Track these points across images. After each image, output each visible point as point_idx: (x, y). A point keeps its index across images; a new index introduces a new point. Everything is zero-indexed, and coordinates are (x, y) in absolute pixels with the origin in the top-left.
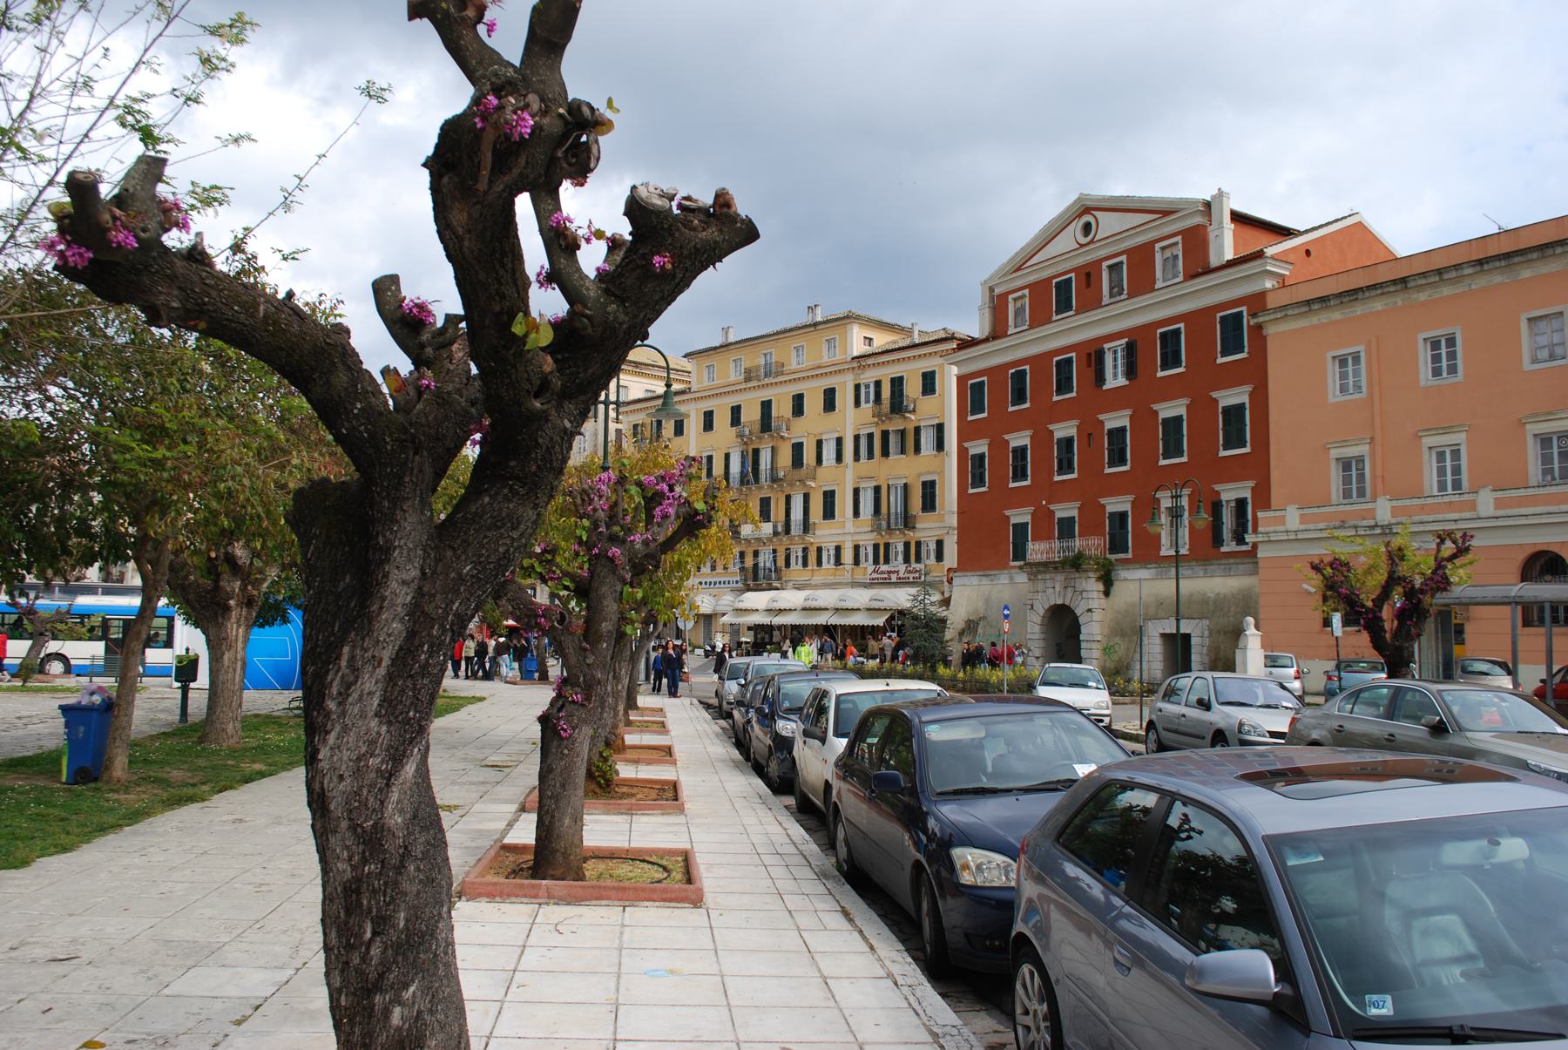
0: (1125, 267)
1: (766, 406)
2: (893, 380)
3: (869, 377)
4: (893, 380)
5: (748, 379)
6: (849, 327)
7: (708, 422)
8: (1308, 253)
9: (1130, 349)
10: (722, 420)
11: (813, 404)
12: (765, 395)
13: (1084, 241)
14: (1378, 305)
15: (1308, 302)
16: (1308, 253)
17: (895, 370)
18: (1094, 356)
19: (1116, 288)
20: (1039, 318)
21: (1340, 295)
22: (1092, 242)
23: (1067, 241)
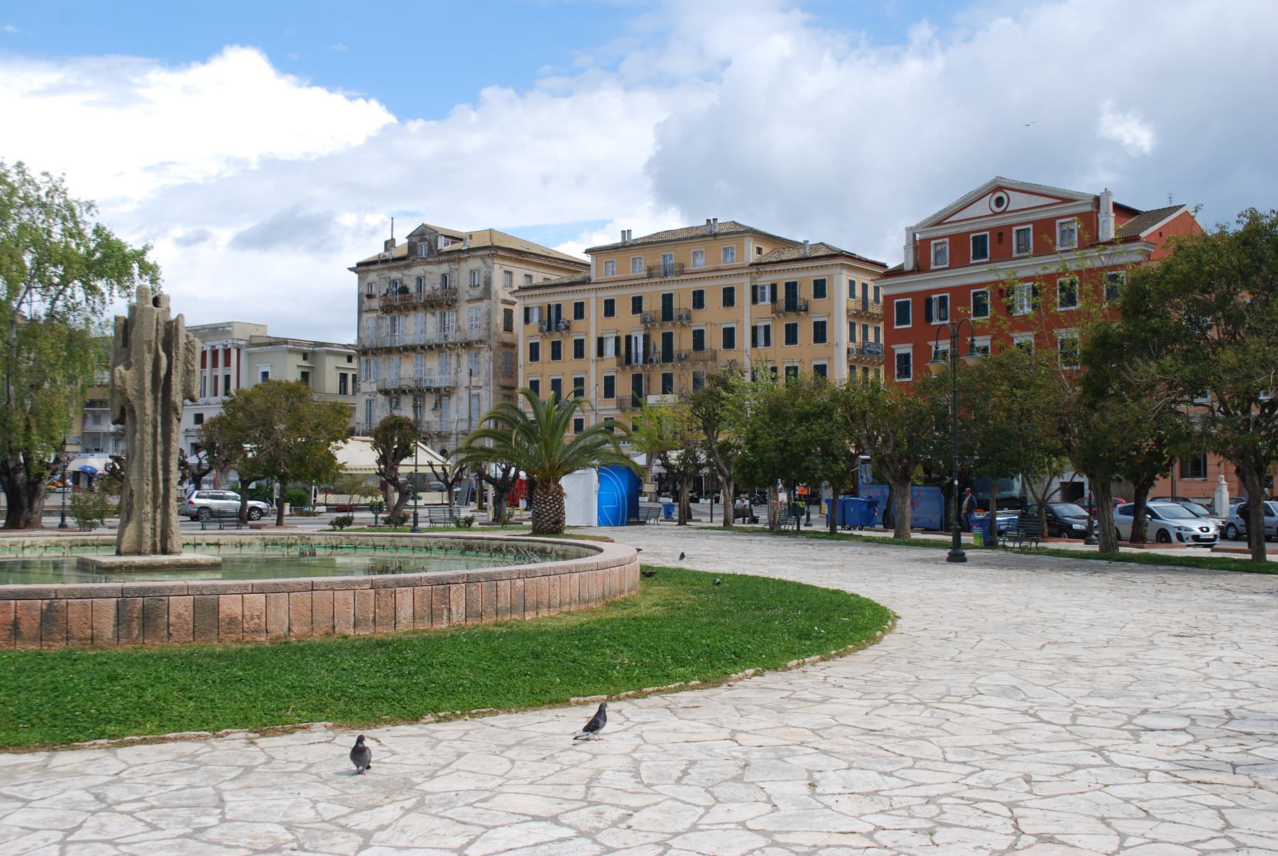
0: (1031, 233)
1: (667, 299)
2: (787, 285)
3: (765, 280)
4: (787, 285)
5: (650, 276)
6: (746, 239)
7: (609, 308)
8: (1161, 234)
11: (714, 299)
12: (667, 289)
13: (997, 210)
16: (1161, 234)
17: (790, 277)
18: (1003, 291)
19: (1022, 247)
20: (958, 261)
23: (983, 208)
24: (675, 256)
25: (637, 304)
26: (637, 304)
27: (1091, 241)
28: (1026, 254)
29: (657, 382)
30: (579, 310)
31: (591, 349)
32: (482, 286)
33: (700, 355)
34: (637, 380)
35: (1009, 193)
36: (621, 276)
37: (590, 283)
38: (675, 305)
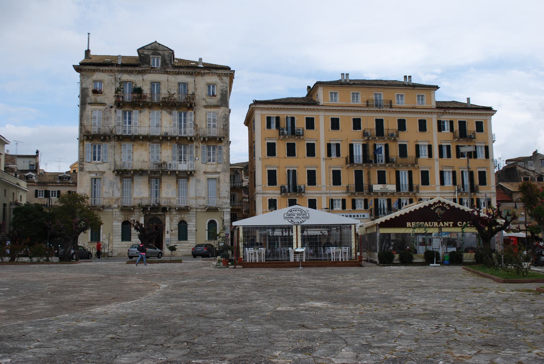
1: (379, 123)
2: (460, 122)
4: (460, 122)
7: (335, 124)
10: (346, 124)
11: (412, 125)
12: (380, 116)
17: (462, 118)
24: (384, 95)
25: (357, 124)
26: (357, 124)
29: (375, 177)
30: (310, 123)
31: (321, 150)
32: (219, 97)
33: (404, 160)
34: (359, 175)
36: (344, 103)
37: (319, 105)
38: (385, 126)
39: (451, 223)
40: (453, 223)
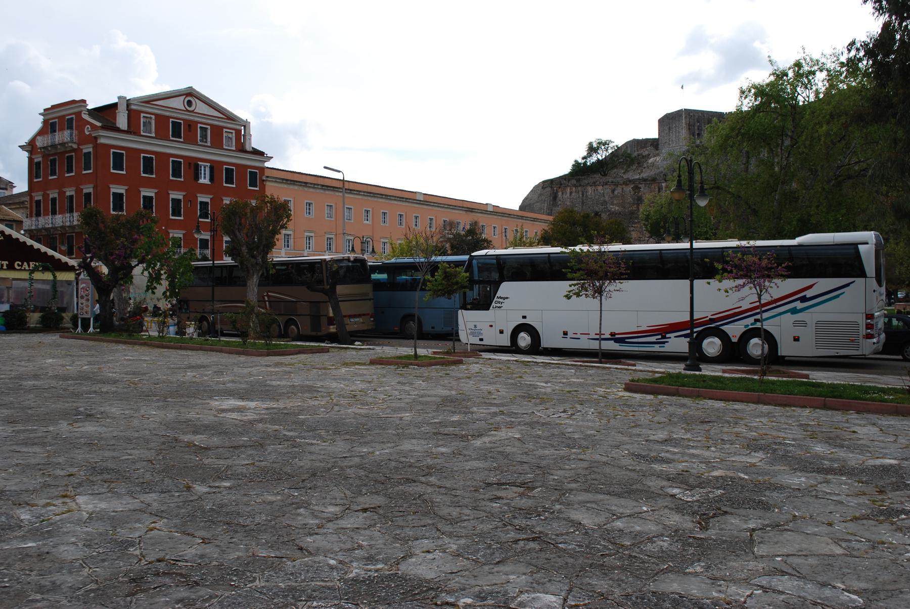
9: (212, 169)
14: (296, 187)
15: (283, 179)
18: (194, 166)
19: (204, 137)
20: (161, 134)
21: (291, 181)
22: (192, 111)
23: (178, 103)
27: (217, 143)
28: (206, 144)
35: (196, 100)
39: (5, 263)
40: (7, 262)
